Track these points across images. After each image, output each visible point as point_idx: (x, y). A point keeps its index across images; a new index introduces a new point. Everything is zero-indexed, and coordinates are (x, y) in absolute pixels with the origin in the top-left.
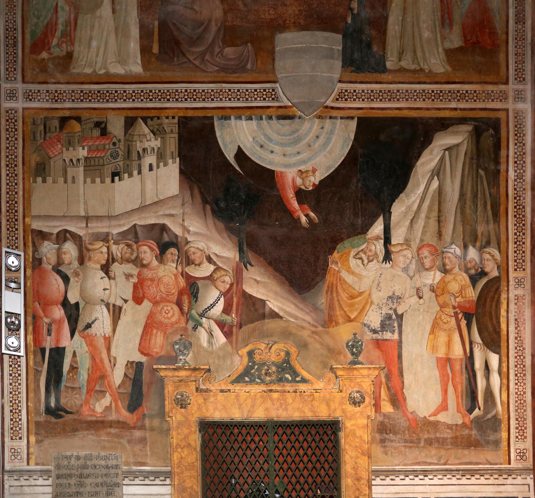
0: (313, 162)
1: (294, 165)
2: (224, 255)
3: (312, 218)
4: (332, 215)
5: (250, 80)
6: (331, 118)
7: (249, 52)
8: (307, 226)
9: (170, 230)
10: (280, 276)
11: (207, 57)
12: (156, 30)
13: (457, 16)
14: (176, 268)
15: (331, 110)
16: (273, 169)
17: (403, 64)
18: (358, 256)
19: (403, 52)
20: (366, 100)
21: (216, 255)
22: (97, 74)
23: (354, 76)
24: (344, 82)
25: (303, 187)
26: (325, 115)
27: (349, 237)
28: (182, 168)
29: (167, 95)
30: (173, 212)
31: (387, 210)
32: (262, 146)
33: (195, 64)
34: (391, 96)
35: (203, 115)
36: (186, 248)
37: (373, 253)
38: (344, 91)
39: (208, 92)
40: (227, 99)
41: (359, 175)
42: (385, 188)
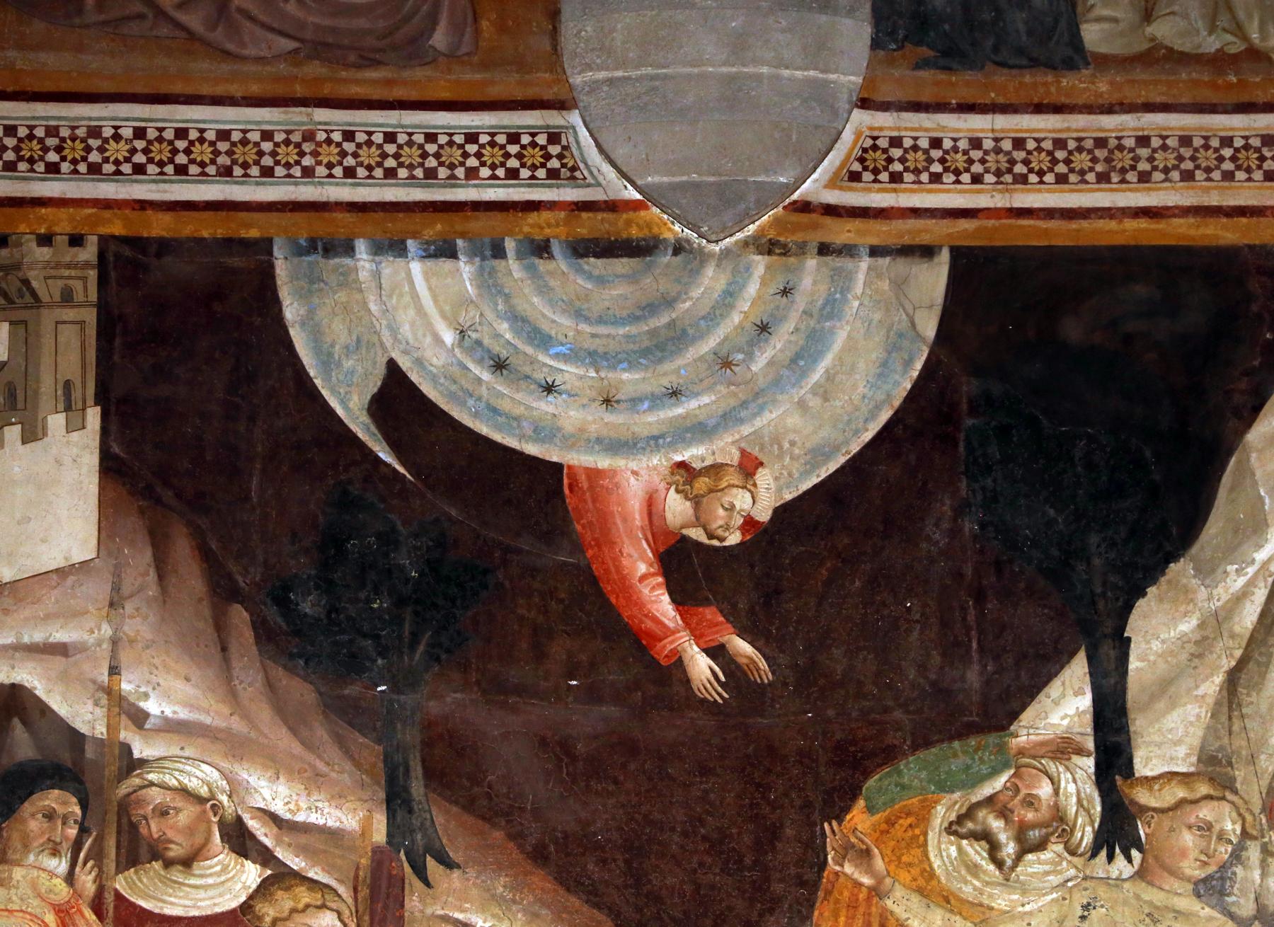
0: (746, 430)
1: (655, 442)
2: (315, 818)
3: (743, 661)
4: (837, 652)
5: (445, 95)
6: (824, 250)
8: (717, 694)
9: (45, 709)
10: (585, 908)
14: (70, 878)
15: (828, 221)
16: (555, 459)
17: (1164, 30)
18: (970, 825)
20: (989, 178)
21: (274, 818)
23: (929, 82)
24: (885, 107)
25: (697, 534)
26: (799, 237)
27: (922, 742)
28: (116, 449)
29: (46, 150)
30: (60, 636)
31: (1109, 630)
32: (499, 366)
34: (1108, 160)
35: (220, 233)
36: (123, 789)
37: (1044, 813)
38: (883, 143)
39: (245, 142)
40: (338, 171)
41: (963, 484)
42: (1094, 539)
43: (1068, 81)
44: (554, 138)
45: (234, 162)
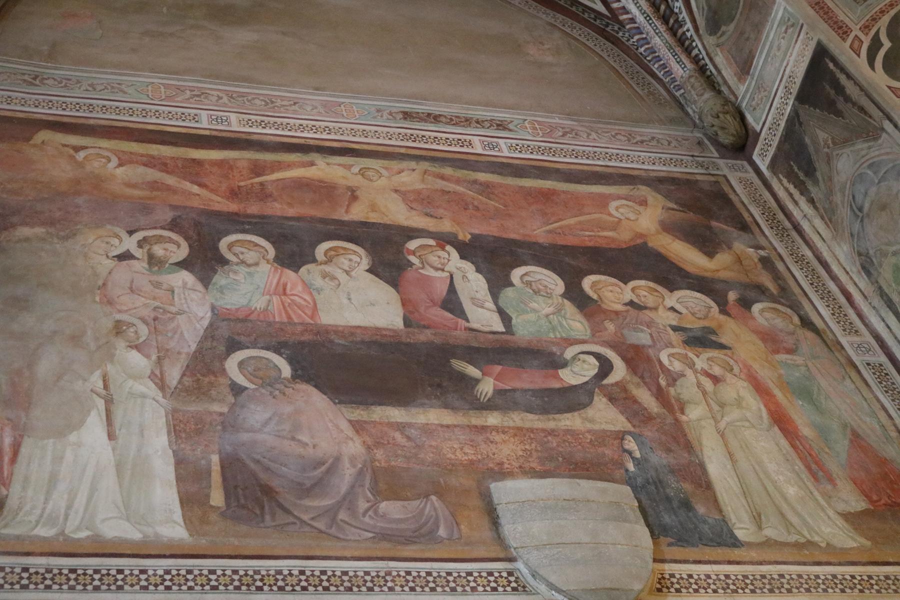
7: (435, 509)
11: (342, 515)
12: (216, 468)
13: (833, 467)
17: (769, 532)
19: (760, 516)
22: (67, 539)
33: (316, 528)
43: (737, 552)
44: (510, 574)
45: (353, 585)
